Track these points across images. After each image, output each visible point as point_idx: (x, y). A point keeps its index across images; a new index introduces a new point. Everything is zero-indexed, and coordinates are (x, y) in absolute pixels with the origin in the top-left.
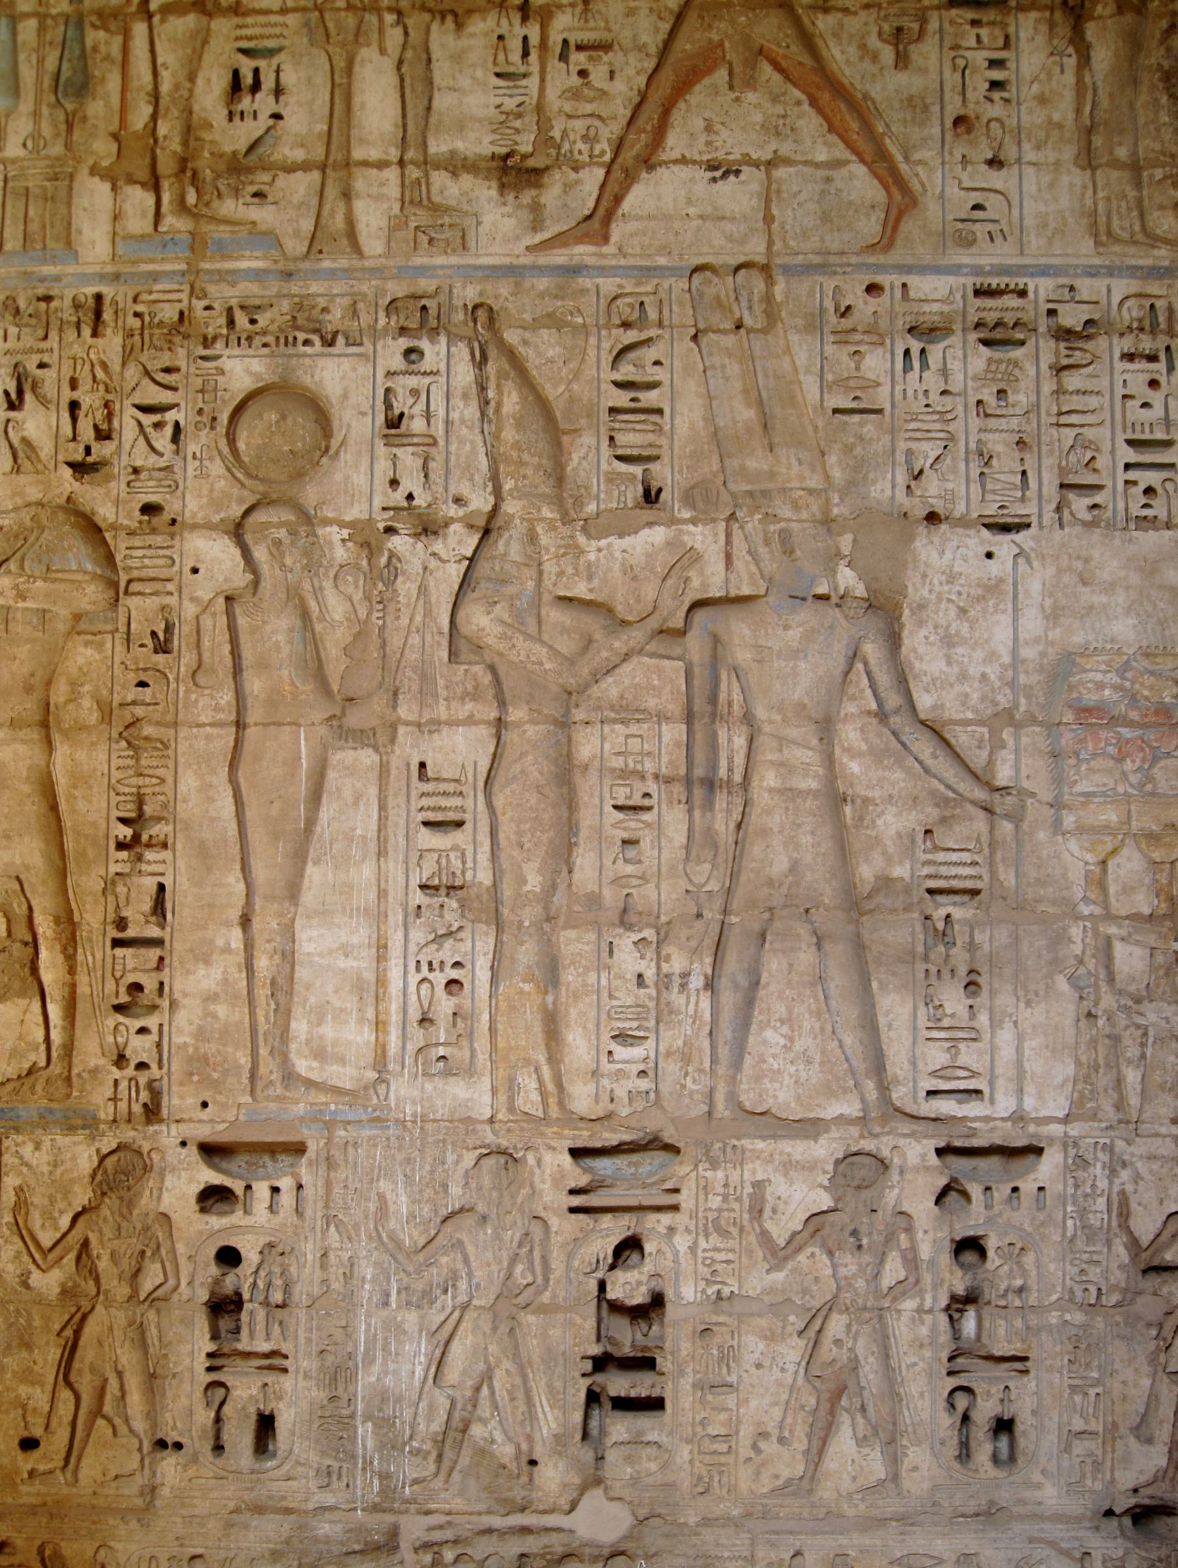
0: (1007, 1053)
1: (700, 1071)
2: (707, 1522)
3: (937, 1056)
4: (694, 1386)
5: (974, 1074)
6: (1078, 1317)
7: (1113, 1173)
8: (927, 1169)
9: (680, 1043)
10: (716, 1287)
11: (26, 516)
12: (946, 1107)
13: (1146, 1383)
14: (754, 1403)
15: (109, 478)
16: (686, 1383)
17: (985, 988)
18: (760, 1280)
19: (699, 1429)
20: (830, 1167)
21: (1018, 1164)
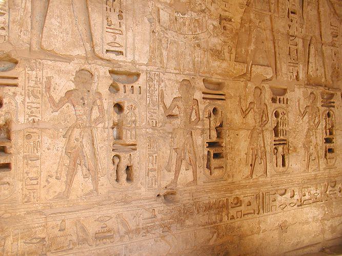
0: (130, 40)
1: (27, 31)
2: (28, 213)
3: (109, 38)
4: (23, 158)
5: (121, 46)
6: (150, 131)
7: (159, 85)
8: (106, 77)
9: (19, 18)
10: (32, 118)
12: (112, 56)
13: (169, 152)
14: (47, 164)
16: (20, 157)
17: (124, 17)
18: (48, 116)
19: (26, 175)
20: (74, 74)
21: (131, 78)
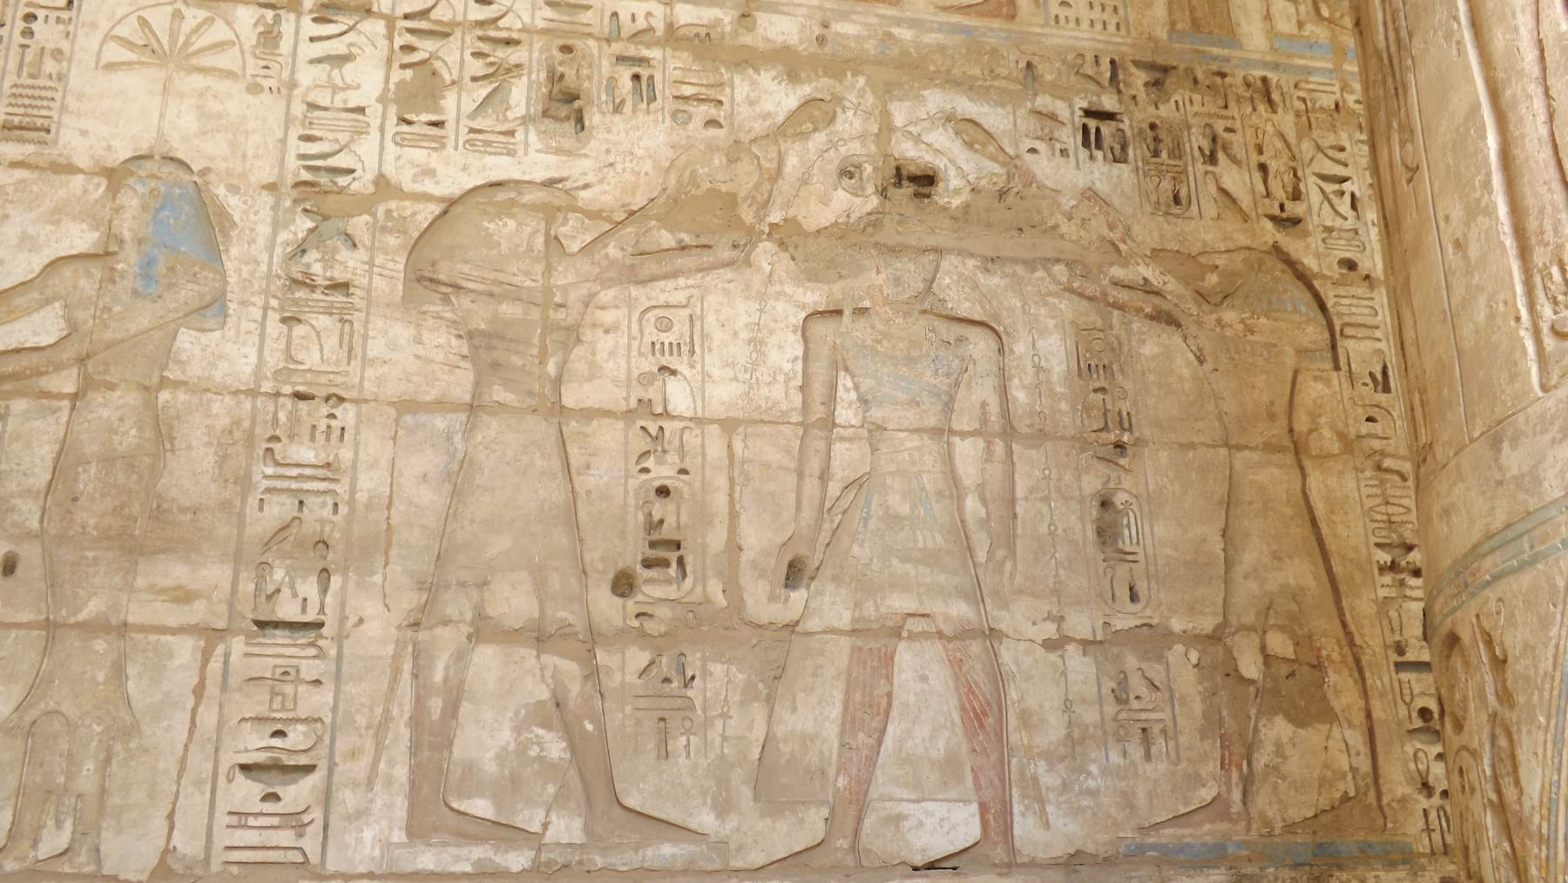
11: (1239, 257)
15: (1306, 234)
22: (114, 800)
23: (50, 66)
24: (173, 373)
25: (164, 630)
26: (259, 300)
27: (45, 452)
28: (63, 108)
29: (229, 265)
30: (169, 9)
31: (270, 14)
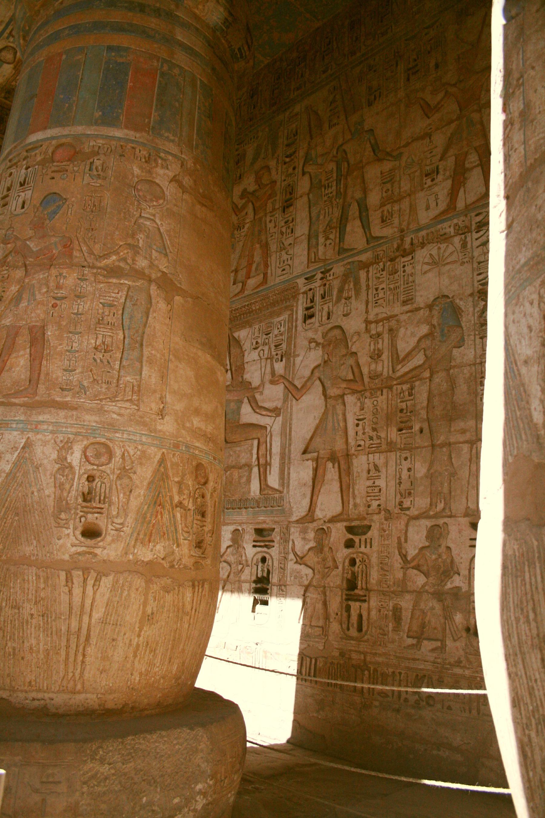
22: (453, 494)
23: (411, 279)
24: (453, 364)
25: (460, 443)
26: (472, 333)
27: (425, 395)
28: (416, 290)
29: (463, 324)
30: (436, 247)
31: (463, 236)
